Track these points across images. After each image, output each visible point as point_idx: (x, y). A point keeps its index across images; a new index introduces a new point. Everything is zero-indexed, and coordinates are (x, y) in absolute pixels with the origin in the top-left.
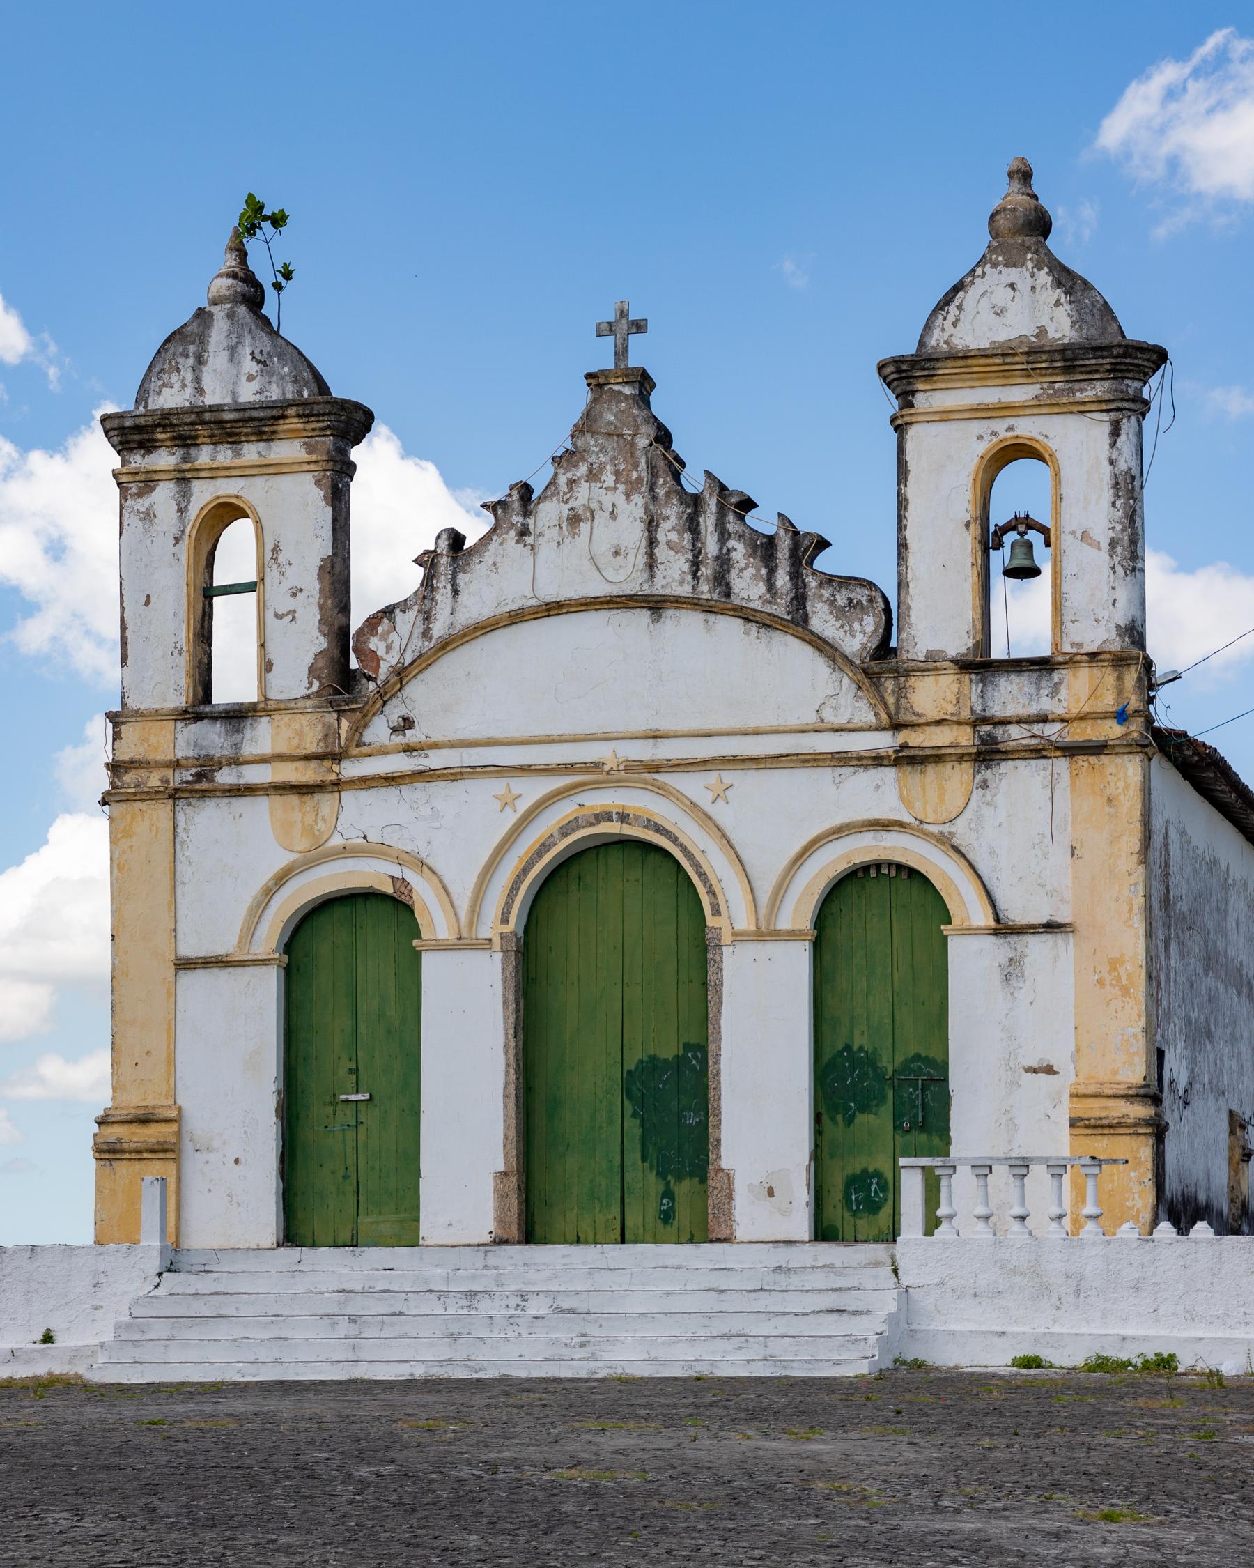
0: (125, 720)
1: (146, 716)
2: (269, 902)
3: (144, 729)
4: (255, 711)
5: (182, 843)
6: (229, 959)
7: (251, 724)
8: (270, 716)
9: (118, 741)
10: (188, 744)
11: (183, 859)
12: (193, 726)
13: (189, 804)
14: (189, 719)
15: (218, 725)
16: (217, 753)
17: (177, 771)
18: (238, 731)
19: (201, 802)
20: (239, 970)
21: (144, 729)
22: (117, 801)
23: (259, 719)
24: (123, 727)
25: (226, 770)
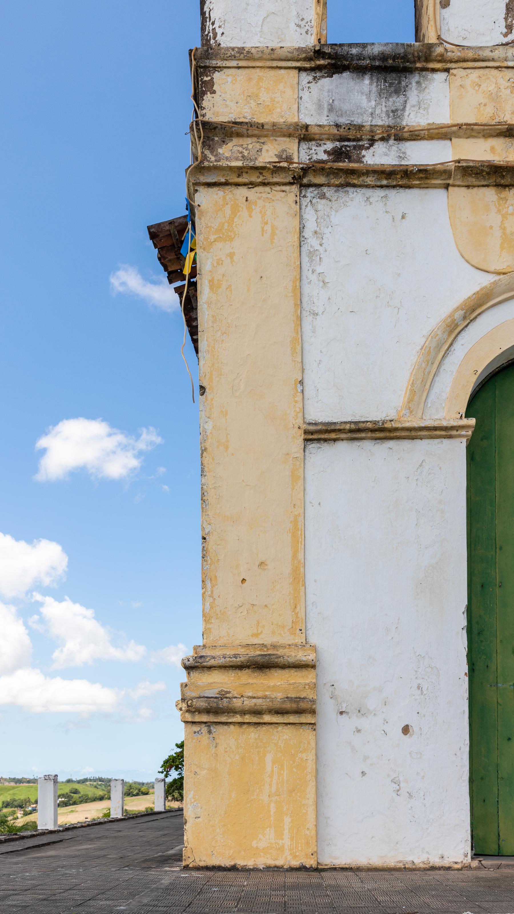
0: (220, 63)
1: (254, 60)
2: (451, 344)
3: (250, 79)
4: (428, 59)
5: (312, 254)
6: (395, 425)
7: (418, 83)
8: (447, 70)
9: (208, 96)
10: (320, 107)
11: (313, 278)
12: (326, 83)
13: (323, 196)
14: (319, 68)
15: (367, 81)
16: (367, 121)
17: (304, 146)
18: (397, 92)
19: (341, 194)
20: (406, 444)
21: (250, 79)
22: (209, 185)
23: (430, 75)
24: (217, 76)
25: (380, 147)
